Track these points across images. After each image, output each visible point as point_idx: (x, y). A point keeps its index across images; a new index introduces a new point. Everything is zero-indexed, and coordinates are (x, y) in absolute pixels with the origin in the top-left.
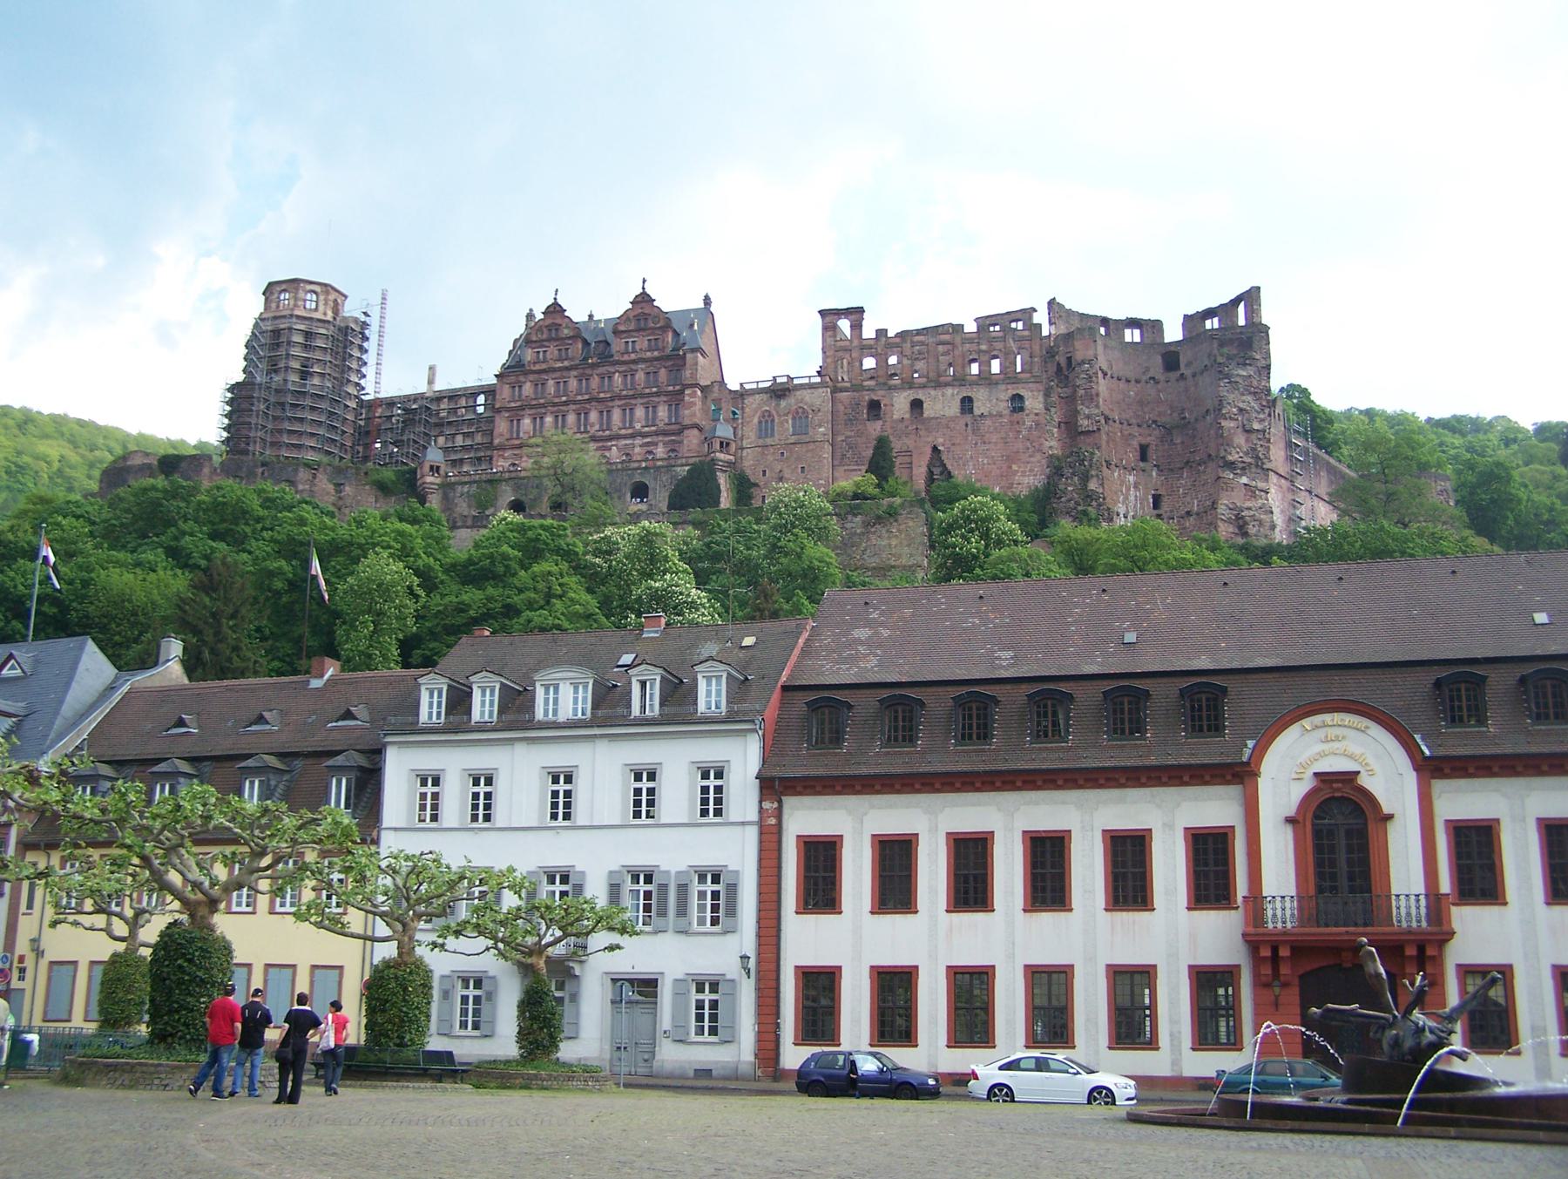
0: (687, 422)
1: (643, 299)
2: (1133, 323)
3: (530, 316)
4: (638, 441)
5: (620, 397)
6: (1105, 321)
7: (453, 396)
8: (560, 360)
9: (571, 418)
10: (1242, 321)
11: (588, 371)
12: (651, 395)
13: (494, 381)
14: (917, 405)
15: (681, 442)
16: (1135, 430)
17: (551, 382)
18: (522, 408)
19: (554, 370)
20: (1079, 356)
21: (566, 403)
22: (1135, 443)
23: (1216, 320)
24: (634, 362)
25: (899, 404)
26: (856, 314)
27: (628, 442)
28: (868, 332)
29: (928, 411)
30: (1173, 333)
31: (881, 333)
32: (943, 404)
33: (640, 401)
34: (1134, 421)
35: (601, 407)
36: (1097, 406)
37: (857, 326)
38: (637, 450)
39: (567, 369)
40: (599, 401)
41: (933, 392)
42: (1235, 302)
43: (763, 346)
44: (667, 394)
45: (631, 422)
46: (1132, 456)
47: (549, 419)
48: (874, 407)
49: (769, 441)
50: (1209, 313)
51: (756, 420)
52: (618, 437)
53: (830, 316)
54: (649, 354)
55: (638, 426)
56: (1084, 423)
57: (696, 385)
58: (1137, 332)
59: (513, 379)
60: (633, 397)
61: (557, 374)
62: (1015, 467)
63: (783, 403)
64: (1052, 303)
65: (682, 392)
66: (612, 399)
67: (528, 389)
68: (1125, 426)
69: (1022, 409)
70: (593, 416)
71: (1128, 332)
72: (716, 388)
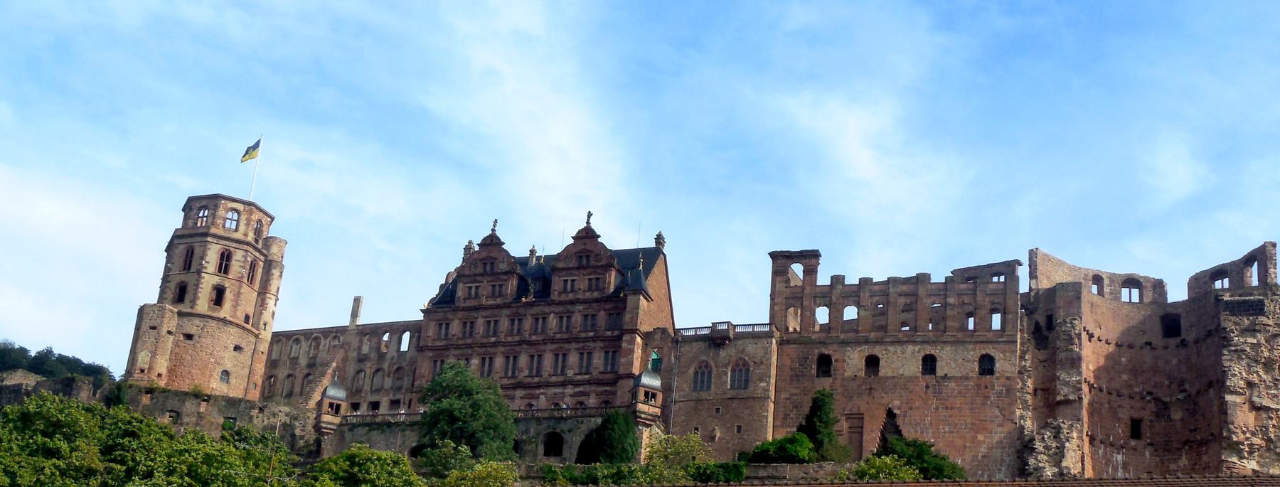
0: (622, 371)
1: (587, 236)
2: (1131, 282)
3: (468, 249)
4: (570, 390)
5: (553, 341)
6: (1097, 279)
7: (375, 331)
8: (493, 296)
9: (499, 362)
10: (1255, 282)
11: (522, 311)
12: (586, 340)
13: (420, 317)
14: (872, 362)
15: (614, 393)
16: (1127, 402)
17: (480, 322)
18: (447, 348)
19: (486, 308)
20: (1060, 316)
21: (495, 345)
22: (1125, 414)
23: (1226, 281)
24: (572, 303)
25: (853, 360)
26: (810, 258)
27: (558, 390)
28: (823, 279)
29: (885, 370)
30: (1177, 293)
31: (837, 280)
32: (901, 362)
33: (574, 345)
34: (1125, 392)
35: (532, 350)
36: (1080, 374)
37: (811, 272)
38: (567, 399)
39: (499, 307)
40: (531, 343)
41: (891, 348)
42: (1249, 260)
43: (715, 290)
44: (604, 339)
45: (563, 367)
46: (1122, 430)
47: (475, 362)
48: (825, 364)
49: (704, 395)
50: (1219, 272)
51: (692, 371)
52: (548, 385)
53: (781, 260)
54: (588, 295)
55: (570, 373)
56: (1063, 392)
57: (634, 331)
58: (1135, 292)
59: (440, 315)
60: (568, 341)
61: (488, 313)
62: (980, 437)
63: (723, 353)
64: (1033, 254)
65: (619, 338)
66: (544, 342)
67: (456, 327)
68: (1114, 397)
69: (991, 372)
70: (523, 360)
71: (1125, 291)
72: (658, 336)
